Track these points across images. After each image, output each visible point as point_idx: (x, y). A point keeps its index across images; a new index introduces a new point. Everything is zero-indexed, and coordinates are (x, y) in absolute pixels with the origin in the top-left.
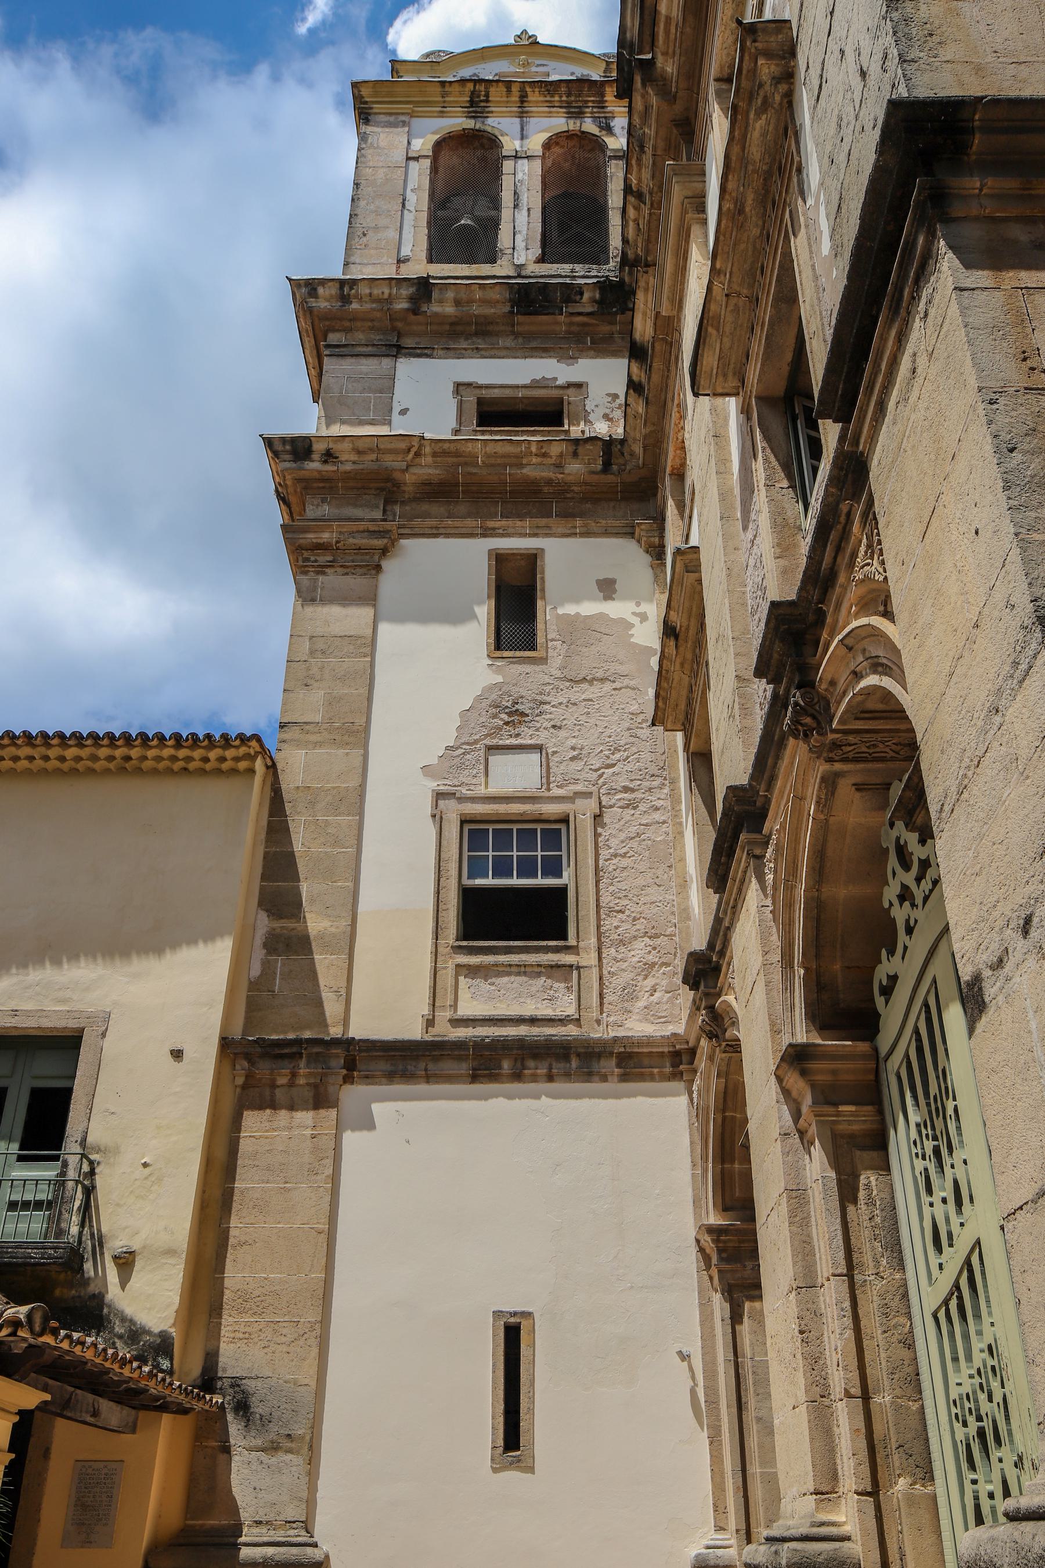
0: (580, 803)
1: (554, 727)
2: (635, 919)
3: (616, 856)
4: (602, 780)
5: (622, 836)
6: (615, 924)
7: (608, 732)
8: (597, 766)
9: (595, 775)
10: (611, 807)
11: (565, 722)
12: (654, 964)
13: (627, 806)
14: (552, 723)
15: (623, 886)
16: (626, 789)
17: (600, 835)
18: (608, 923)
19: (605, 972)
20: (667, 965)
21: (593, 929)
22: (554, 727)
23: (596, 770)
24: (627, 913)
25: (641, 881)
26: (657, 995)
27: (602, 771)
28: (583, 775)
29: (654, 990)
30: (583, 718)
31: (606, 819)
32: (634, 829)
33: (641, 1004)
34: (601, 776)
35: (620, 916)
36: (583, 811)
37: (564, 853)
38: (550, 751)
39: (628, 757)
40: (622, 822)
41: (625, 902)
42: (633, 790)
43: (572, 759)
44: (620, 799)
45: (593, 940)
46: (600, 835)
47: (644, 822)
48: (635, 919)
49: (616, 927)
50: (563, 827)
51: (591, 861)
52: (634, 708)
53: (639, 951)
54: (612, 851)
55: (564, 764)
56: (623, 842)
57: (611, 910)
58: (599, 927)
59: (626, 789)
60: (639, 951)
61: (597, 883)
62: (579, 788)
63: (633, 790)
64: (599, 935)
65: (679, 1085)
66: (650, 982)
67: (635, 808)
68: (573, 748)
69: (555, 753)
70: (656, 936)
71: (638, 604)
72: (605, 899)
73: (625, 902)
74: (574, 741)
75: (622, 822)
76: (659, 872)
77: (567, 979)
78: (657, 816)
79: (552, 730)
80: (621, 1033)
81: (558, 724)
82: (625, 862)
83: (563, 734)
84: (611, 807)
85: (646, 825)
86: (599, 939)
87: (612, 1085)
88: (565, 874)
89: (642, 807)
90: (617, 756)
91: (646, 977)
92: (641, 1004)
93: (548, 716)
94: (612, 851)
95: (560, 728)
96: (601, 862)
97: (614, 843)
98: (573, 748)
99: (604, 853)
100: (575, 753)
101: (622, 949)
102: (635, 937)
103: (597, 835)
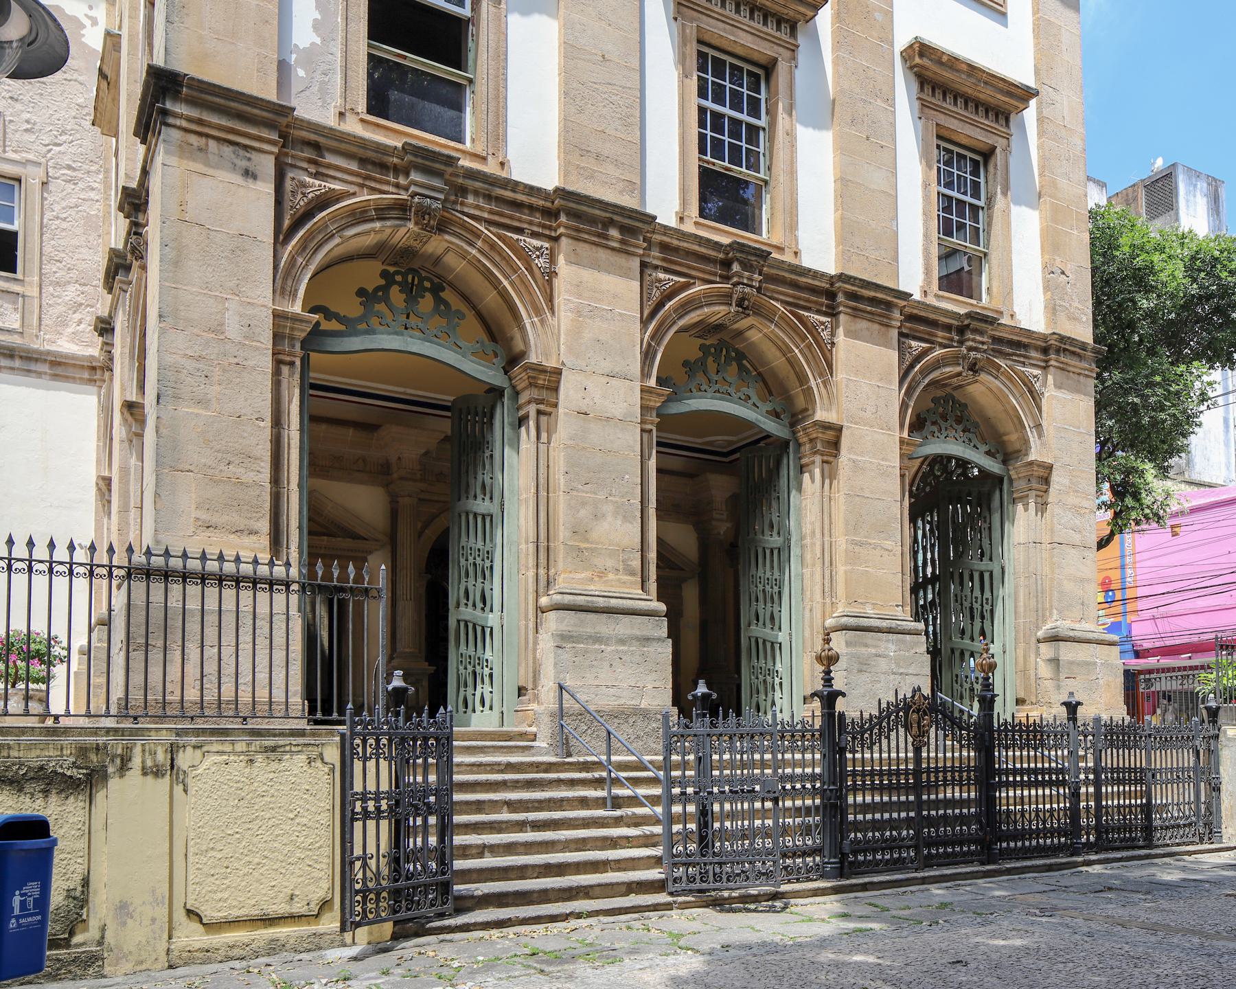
0: (31, 169)
1: (11, 98)
2: (69, 269)
3: (58, 218)
4: (49, 155)
5: (64, 204)
6: (54, 270)
7: (57, 116)
8: (47, 142)
9: (45, 149)
10: (56, 178)
11: (21, 97)
12: (81, 304)
13: (70, 181)
14: (10, 94)
15: (62, 242)
16: (69, 167)
17: (46, 199)
18: (47, 268)
19: (44, 303)
20: (92, 307)
21: (36, 270)
22: (11, 98)
23: (46, 145)
24: (64, 263)
25: (75, 242)
26: (82, 326)
27: (50, 147)
28: (35, 147)
29: (79, 322)
30: (37, 97)
31: (51, 187)
32: (73, 201)
33: (70, 330)
34: (50, 151)
35: (58, 264)
36: (33, 177)
37: (16, 205)
38: (7, 119)
39: (72, 141)
40: (65, 193)
41: (63, 255)
42: (74, 169)
43: (26, 130)
44: (64, 174)
45: (36, 278)
46: (46, 199)
47: (82, 197)
48: (69, 269)
49: (55, 272)
50: (16, 184)
51: (37, 218)
52: (81, 101)
53: (71, 292)
54: (55, 214)
55: (19, 133)
56: (64, 208)
57: (51, 259)
58: (41, 269)
59: (69, 167)
60: (71, 292)
61: (42, 235)
62: (31, 157)
63: (74, 169)
64: (41, 275)
65: (95, 389)
66: (77, 316)
67: (75, 184)
68: (28, 122)
69: (11, 121)
70: (85, 285)
71: (91, 8)
72: (47, 250)
73: (63, 255)
74: (28, 115)
75: (65, 193)
76: (91, 238)
77: (15, 303)
78: (92, 195)
79: (10, 101)
80: (53, 348)
81: (16, 97)
82: (64, 225)
83: (18, 106)
84: (56, 178)
85: (84, 200)
86: (40, 279)
87: (44, 381)
88: (16, 222)
89: (81, 185)
90: (64, 138)
91: (75, 312)
92: (70, 330)
93: (7, 88)
94: (55, 214)
95: (17, 100)
96: (45, 221)
97: (57, 207)
98: (28, 122)
99: (48, 215)
100: (29, 126)
101: (58, 289)
102: (69, 283)
103: (43, 199)
